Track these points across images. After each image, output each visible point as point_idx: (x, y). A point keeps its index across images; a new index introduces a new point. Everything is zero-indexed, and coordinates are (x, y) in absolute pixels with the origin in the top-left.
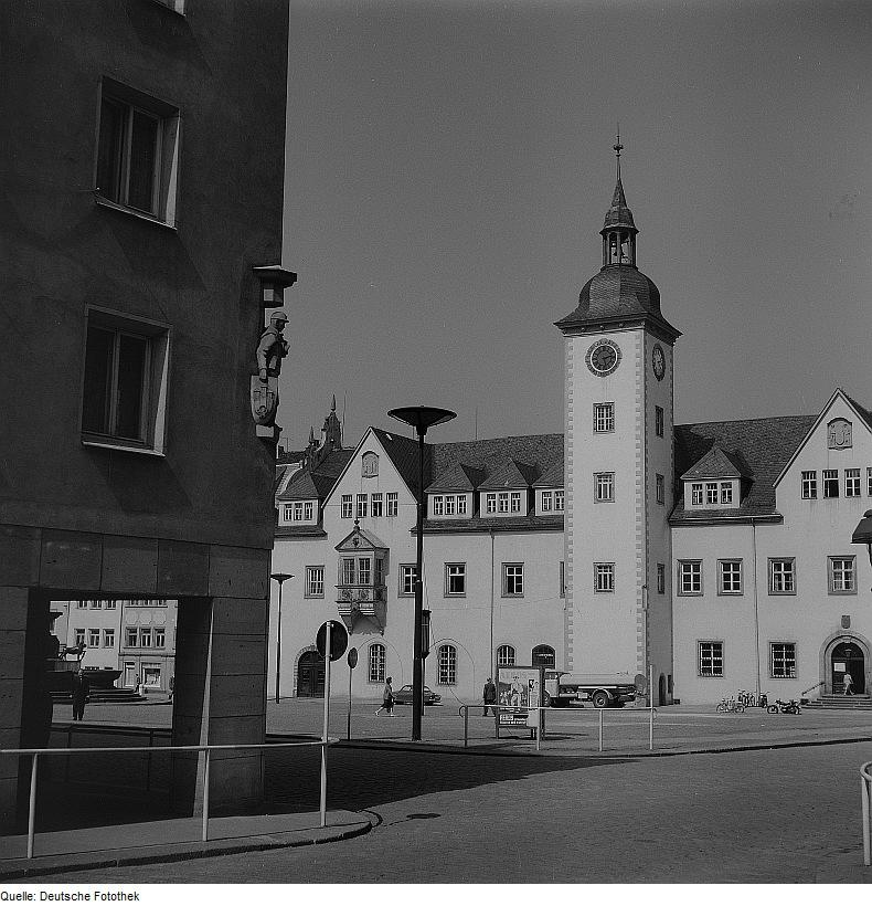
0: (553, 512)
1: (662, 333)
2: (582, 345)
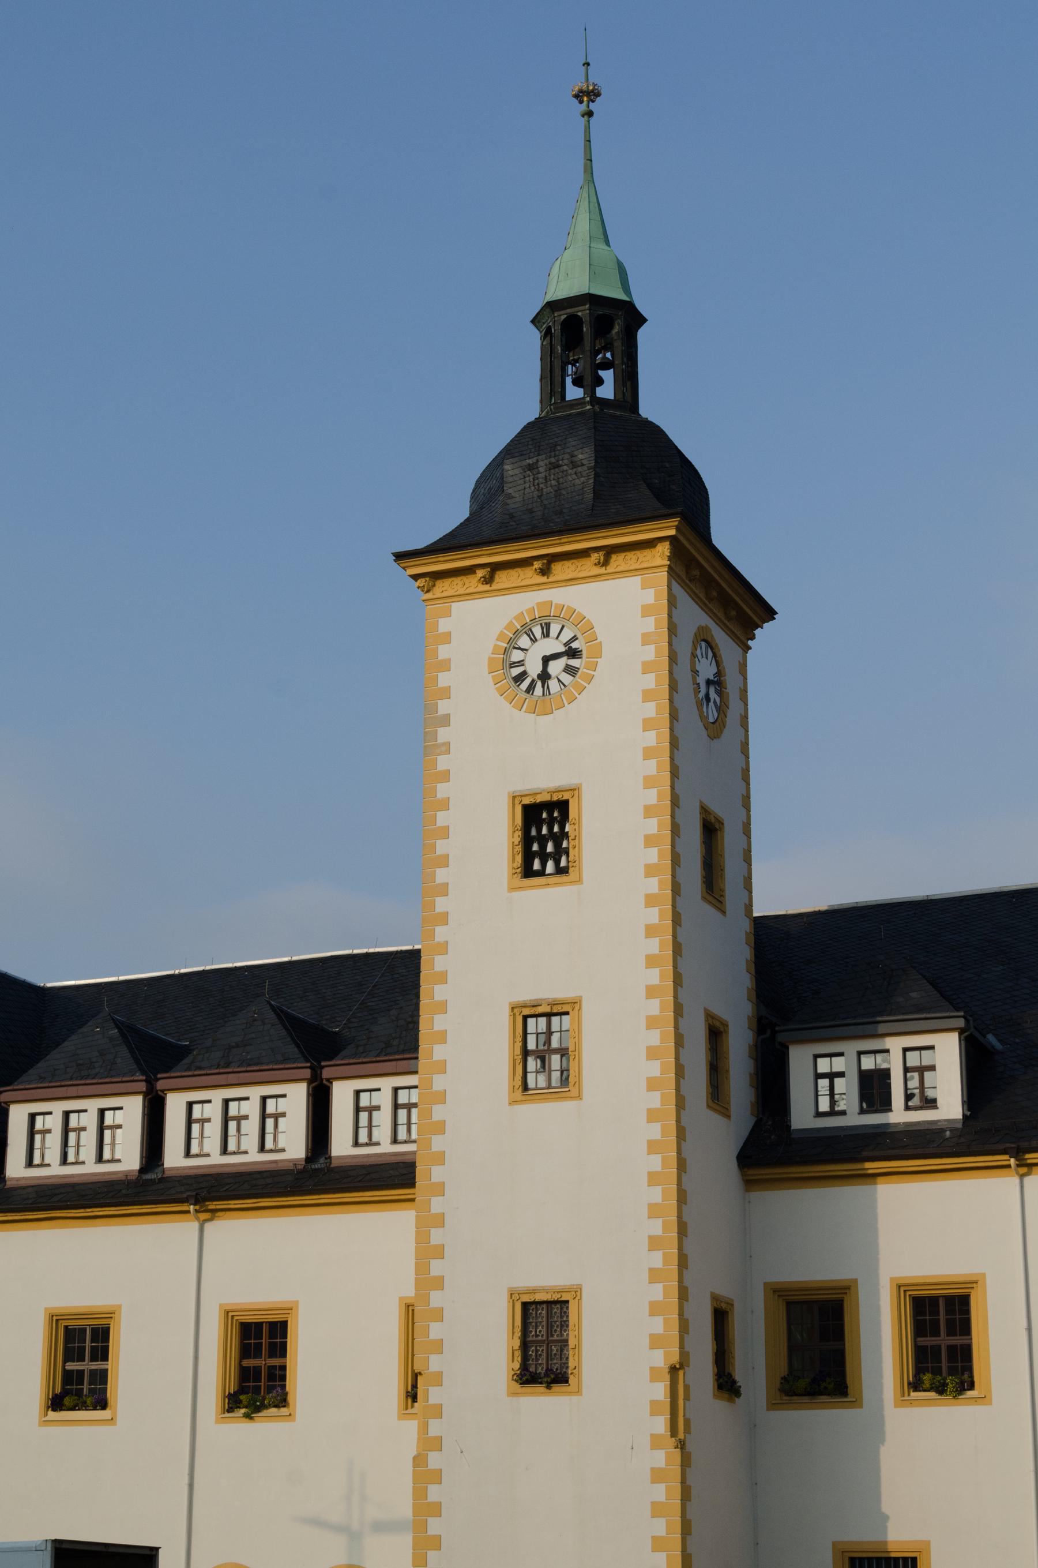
0: (386, 1147)
1: (723, 602)
2: (476, 621)
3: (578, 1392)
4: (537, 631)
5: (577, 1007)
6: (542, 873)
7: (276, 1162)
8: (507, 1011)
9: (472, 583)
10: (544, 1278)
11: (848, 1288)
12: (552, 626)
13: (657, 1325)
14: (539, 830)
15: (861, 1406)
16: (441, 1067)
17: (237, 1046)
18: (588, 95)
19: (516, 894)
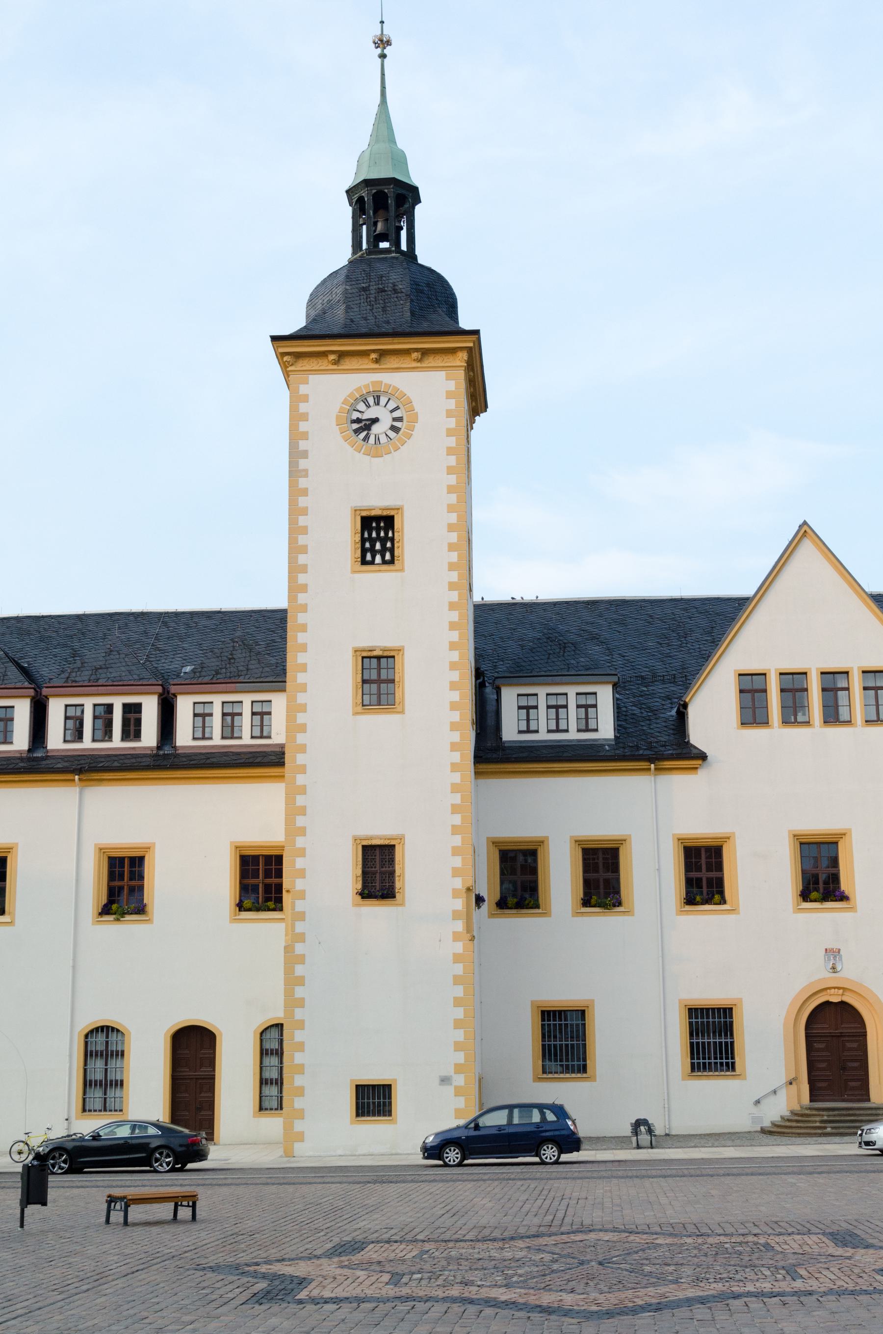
3: (402, 904)
4: (371, 400)
5: (401, 653)
6: (372, 562)
7: (134, 748)
8: (350, 653)
9: (323, 364)
10: (378, 831)
11: (543, 842)
12: (381, 398)
13: (458, 862)
14: (370, 534)
15: (550, 916)
16: (303, 688)
17: (101, 668)
18: (382, 43)
19: (357, 576)
